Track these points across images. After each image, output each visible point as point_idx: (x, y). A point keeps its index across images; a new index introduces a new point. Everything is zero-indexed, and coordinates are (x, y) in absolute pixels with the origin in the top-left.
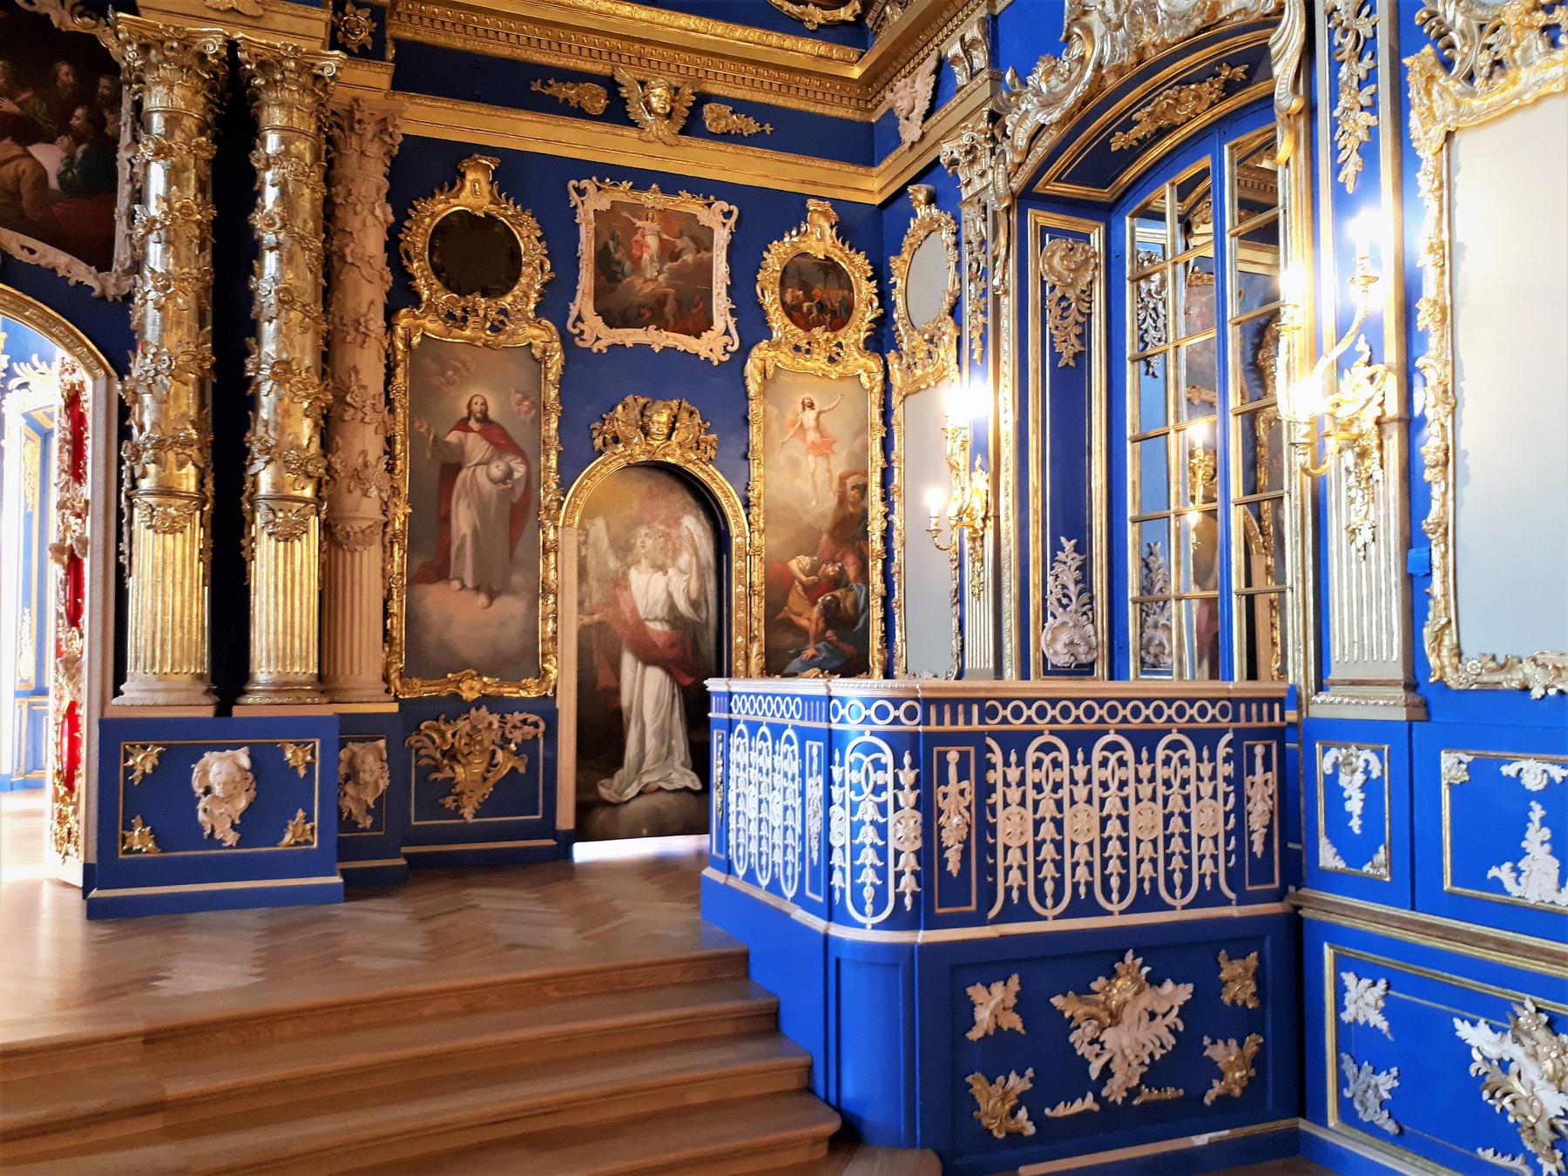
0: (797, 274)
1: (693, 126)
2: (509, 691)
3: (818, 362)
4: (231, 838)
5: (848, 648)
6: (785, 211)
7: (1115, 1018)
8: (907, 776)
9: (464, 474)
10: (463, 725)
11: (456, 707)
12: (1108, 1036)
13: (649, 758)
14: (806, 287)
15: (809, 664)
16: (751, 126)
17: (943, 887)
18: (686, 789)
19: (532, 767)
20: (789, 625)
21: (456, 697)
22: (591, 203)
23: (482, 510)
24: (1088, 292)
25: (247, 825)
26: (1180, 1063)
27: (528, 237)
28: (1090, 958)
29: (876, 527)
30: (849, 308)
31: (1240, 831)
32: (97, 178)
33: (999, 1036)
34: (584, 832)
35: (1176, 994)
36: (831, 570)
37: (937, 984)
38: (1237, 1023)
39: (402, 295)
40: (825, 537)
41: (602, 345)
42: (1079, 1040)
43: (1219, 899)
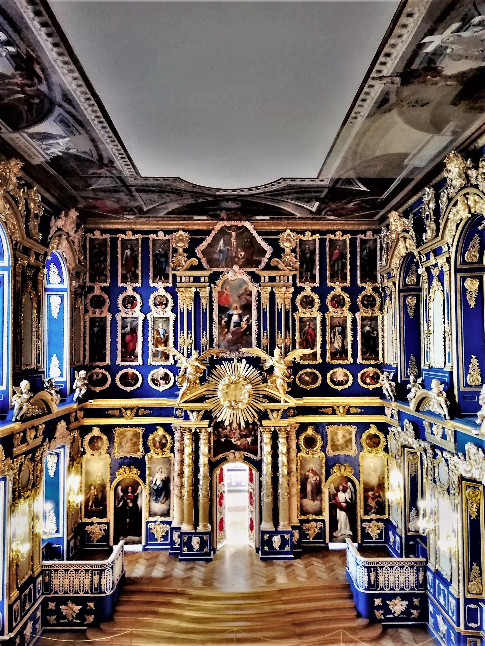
0: (370, 437)
1: (348, 413)
2: (317, 518)
4: (278, 549)
6: (365, 426)
7: (396, 605)
8: (366, 571)
9: (309, 480)
10: (310, 524)
11: (308, 521)
12: (395, 607)
13: (343, 528)
14: (371, 439)
15: (374, 513)
16: (359, 410)
17: (370, 586)
18: (350, 535)
19: (321, 531)
21: (308, 519)
22: (330, 430)
23: (312, 486)
24: (416, 464)
26: (407, 612)
27: (319, 437)
28: (393, 596)
29: (386, 486)
30: (379, 442)
31: (418, 580)
32: (255, 442)
33: (379, 606)
34: (331, 541)
35: (405, 603)
36: (377, 494)
37: (371, 598)
38: (415, 607)
39: (299, 450)
40: (376, 488)
41: (332, 455)
42: (391, 607)
43: (413, 589)
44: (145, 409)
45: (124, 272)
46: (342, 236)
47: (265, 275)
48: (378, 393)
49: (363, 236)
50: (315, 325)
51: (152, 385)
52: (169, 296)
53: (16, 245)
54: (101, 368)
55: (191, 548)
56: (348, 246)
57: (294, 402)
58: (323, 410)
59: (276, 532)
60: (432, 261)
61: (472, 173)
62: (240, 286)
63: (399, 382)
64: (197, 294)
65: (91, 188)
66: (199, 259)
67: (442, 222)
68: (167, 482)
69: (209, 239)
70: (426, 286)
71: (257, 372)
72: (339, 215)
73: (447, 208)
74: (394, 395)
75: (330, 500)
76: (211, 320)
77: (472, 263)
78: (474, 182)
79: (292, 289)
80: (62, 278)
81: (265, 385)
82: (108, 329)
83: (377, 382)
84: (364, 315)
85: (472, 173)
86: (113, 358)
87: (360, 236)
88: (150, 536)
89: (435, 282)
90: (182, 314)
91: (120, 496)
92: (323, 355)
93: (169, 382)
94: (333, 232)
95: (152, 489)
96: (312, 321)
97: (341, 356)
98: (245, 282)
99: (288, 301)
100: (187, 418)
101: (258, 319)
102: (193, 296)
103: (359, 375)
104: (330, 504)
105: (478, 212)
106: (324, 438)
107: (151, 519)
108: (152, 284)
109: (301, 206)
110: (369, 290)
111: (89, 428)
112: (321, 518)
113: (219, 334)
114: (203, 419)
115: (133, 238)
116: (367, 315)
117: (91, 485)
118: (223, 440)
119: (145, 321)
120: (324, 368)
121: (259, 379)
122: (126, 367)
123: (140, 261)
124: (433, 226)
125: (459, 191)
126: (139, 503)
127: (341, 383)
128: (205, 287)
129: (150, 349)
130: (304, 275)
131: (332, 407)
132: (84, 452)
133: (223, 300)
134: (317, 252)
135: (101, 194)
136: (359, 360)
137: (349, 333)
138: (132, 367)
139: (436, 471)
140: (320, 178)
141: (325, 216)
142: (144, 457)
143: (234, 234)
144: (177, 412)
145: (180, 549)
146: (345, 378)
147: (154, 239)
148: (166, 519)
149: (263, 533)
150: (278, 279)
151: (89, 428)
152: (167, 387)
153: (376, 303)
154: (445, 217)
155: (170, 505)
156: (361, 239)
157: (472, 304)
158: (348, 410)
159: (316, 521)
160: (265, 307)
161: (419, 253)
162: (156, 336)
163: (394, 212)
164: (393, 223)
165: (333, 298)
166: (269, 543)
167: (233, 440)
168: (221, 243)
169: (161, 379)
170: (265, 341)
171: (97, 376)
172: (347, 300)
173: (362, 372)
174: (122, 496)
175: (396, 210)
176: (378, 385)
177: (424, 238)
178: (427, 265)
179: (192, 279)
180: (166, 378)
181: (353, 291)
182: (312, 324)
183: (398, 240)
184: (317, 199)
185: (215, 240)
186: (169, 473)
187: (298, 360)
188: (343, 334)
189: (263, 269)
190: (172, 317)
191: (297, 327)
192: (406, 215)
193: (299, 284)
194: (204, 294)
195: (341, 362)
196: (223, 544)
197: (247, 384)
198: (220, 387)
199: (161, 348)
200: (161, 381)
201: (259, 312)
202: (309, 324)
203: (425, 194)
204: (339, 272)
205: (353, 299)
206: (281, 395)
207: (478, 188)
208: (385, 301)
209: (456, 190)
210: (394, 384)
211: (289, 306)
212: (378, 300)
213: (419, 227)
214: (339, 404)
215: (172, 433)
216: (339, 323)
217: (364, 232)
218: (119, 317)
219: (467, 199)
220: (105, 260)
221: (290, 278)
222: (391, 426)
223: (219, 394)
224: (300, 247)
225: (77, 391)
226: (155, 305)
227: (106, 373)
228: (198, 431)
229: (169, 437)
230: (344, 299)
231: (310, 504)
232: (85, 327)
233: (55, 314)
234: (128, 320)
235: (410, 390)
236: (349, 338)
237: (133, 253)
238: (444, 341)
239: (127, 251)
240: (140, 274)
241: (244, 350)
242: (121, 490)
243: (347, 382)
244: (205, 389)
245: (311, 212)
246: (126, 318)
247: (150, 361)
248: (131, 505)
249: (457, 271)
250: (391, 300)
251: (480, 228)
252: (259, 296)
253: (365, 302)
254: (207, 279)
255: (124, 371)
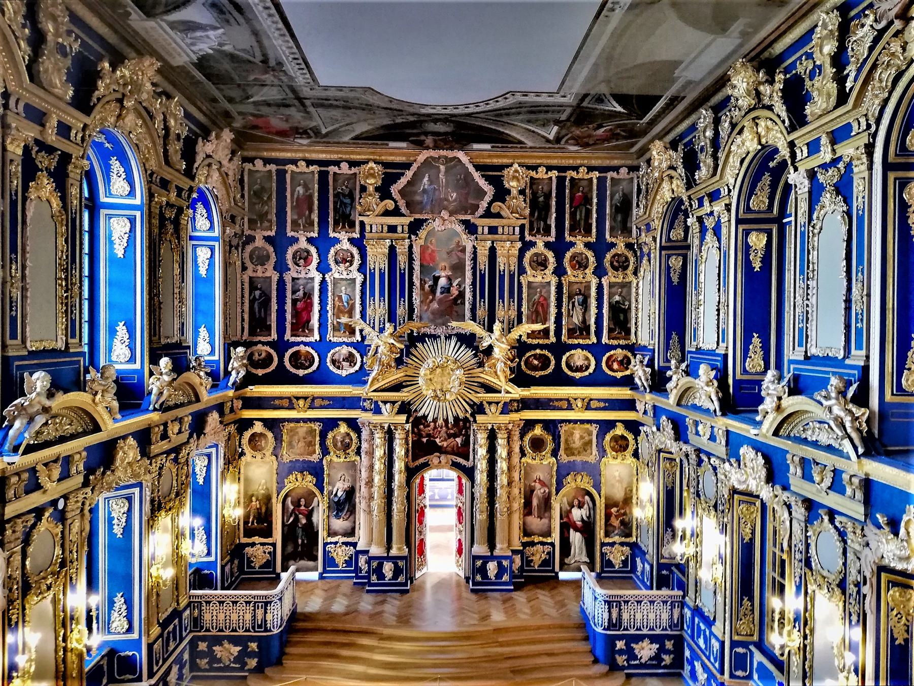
0: (615, 439)
1: (588, 408)
2: (545, 540)
3: (619, 460)
5: (627, 531)
6: (611, 424)
14: (616, 441)
15: (617, 534)
16: (602, 405)
20: (611, 525)
22: (563, 429)
24: (674, 473)
25: (497, 576)
27: (549, 438)
29: (634, 501)
30: (627, 446)
32: (466, 443)
34: (561, 569)
36: (622, 511)
39: (523, 454)
44: (323, 398)
45: (296, 217)
46: (588, 173)
47: (483, 224)
48: (628, 382)
49: (614, 175)
50: (549, 292)
51: (331, 368)
52: (355, 251)
53: (151, 175)
54: (264, 344)
55: (381, 576)
56: (595, 187)
57: (518, 393)
58: (556, 404)
59: (492, 558)
60: (707, 208)
61: (765, 89)
62: (449, 239)
63: (656, 368)
64: (392, 249)
65: (252, 100)
66: (396, 202)
67: (721, 155)
68: (350, 493)
69: (409, 174)
70: (697, 242)
71: (470, 353)
72: (585, 145)
73: (729, 137)
74: (649, 386)
75: (561, 518)
76: (411, 284)
77: (759, 212)
78: (766, 101)
79: (519, 245)
80: (212, 223)
81: (480, 369)
82: (274, 294)
83: (627, 369)
84: (613, 280)
85: (765, 89)
86: (281, 330)
87: (610, 175)
88: (329, 561)
89: (709, 236)
90: (372, 275)
91: (290, 510)
92: (558, 333)
93: (355, 364)
94: (576, 168)
95: (332, 503)
96: (544, 287)
97: (581, 334)
98: (457, 234)
99: (514, 261)
100: (378, 411)
101: (474, 284)
102: (387, 251)
103: (605, 359)
104: (561, 524)
105: (770, 142)
106: (556, 438)
107: (329, 540)
108: (332, 235)
109: (533, 132)
110: (621, 248)
111: (249, 423)
112: (549, 540)
113: (421, 302)
114: (399, 412)
115: (307, 170)
116: (617, 280)
117: (252, 496)
118: (425, 440)
119: (323, 282)
120: (559, 349)
121: (473, 362)
122: (298, 344)
123: (316, 202)
124: (710, 161)
125: (746, 114)
126: (314, 519)
127: (579, 369)
128: (403, 239)
129: (330, 321)
130: (535, 225)
131: (568, 400)
132: (242, 454)
133: (427, 256)
134: (554, 195)
135: (265, 110)
136: (605, 340)
137: (593, 303)
138: (306, 344)
139: (701, 481)
140: (562, 93)
141: (566, 146)
142: (322, 459)
143: (442, 168)
144: (365, 404)
145: (368, 577)
146: (586, 362)
147: (335, 173)
148: (350, 540)
149: (475, 558)
150: (500, 230)
151: (249, 423)
152: (352, 370)
153: (628, 266)
154: (727, 149)
155: (355, 522)
156: (612, 179)
157: (757, 265)
158: (589, 403)
159: (543, 544)
160: (483, 267)
161: (690, 198)
162: (337, 303)
163: (657, 143)
164: (656, 156)
165: (573, 257)
166: (483, 571)
167: (438, 440)
168: (426, 179)
169: (344, 360)
170: (482, 312)
171: (260, 355)
172: (592, 259)
173: (608, 355)
174: (293, 510)
175: (660, 139)
176: (628, 373)
177: (697, 177)
178: (699, 214)
179: (386, 228)
180: (350, 359)
181: (600, 248)
182: (544, 291)
183: (662, 180)
184: (557, 122)
185: (417, 177)
186: (355, 481)
187: (524, 338)
188: (585, 304)
189: (481, 217)
190: (359, 278)
191: (525, 295)
192: (674, 145)
193: (528, 238)
194: (402, 250)
195: (581, 341)
196: (424, 571)
197: (458, 368)
198: (422, 372)
199: (344, 320)
200: (344, 363)
201: (474, 274)
202: (541, 291)
203: (700, 118)
204: (582, 223)
205: (599, 259)
206: (501, 382)
207: (772, 110)
208: (641, 262)
209: (743, 113)
210: (649, 370)
211: (514, 267)
212: (632, 260)
213: (691, 163)
214: (575, 396)
215: (358, 431)
216: (580, 290)
217: (616, 169)
218: (288, 277)
219: (757, 124)
220: (270, 198)
221: (517, 229)
222: (643, 425)
223: (421, 381)
224: (531, 187)
225: (234, 373)
226: (337, 262)
227: (272, 351)
228: (393, 428)
229: (354, 435)
230: (587, 258)
231: (535, 522)
232: (243, 289)
233: (203, 271)
234: (301, 282)
235: (670, 378)
236: (593, 310)
237: (307, 191)
238: (718, 315)
239: (298, 188)
240: (316, 220)
241: (454, 324)
242: (292, 502)
243: (587, 368)
244: (402, 374)
245: (548, 141)
246: (298, 279)
247: (330, 337)
248: (304, 521)
249: (739, 221)
250: (649, 261)
251: (771, 164)
252: (475, 253)
253: (615, 263)
254: (406, 228)
255: (295, 349)
